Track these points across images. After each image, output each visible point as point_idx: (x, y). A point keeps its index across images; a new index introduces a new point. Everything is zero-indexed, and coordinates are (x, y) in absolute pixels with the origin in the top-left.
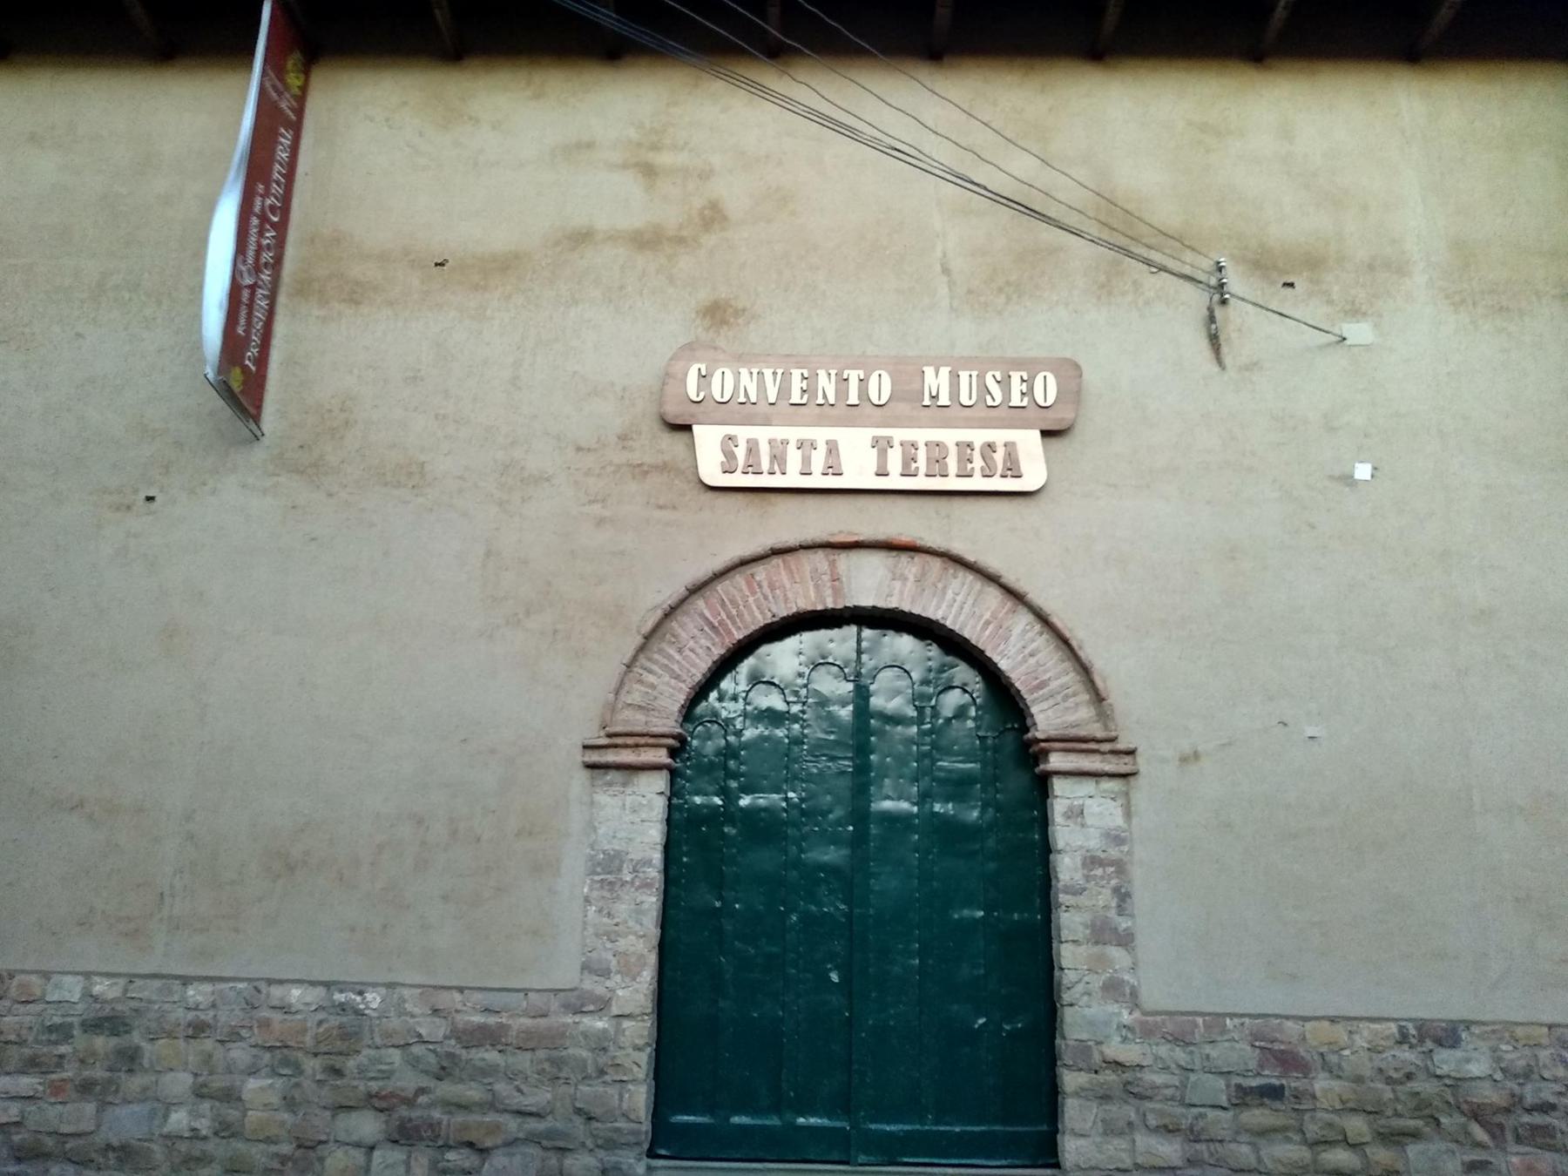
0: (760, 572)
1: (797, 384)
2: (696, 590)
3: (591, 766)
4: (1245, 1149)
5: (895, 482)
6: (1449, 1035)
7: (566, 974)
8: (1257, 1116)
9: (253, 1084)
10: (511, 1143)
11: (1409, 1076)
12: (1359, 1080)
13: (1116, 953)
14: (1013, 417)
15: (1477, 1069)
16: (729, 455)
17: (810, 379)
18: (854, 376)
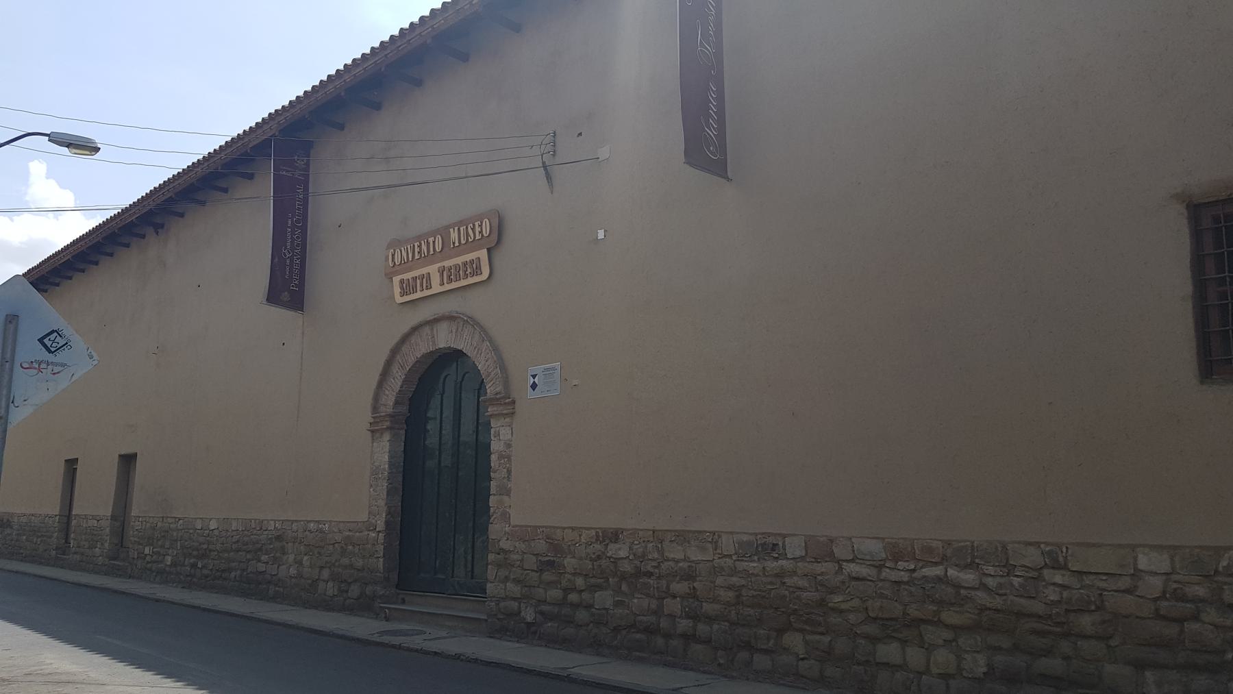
0: (413, 339)
1: (417, 250)
2: (395, 351)
3: (373, 431)
4: (541, 590)
5: (448, 287)
6: (614, 536)
7: (364, 517)
8: (547, 576)
9: (306, 558)
10: (355, 581)
11: (599, 557)
12: (581, 559)
13: (505, 498)
14: (472, 245)
15: (622, 554)
16: (402, 288)
17: (420, 246)
18: (431, 240)
